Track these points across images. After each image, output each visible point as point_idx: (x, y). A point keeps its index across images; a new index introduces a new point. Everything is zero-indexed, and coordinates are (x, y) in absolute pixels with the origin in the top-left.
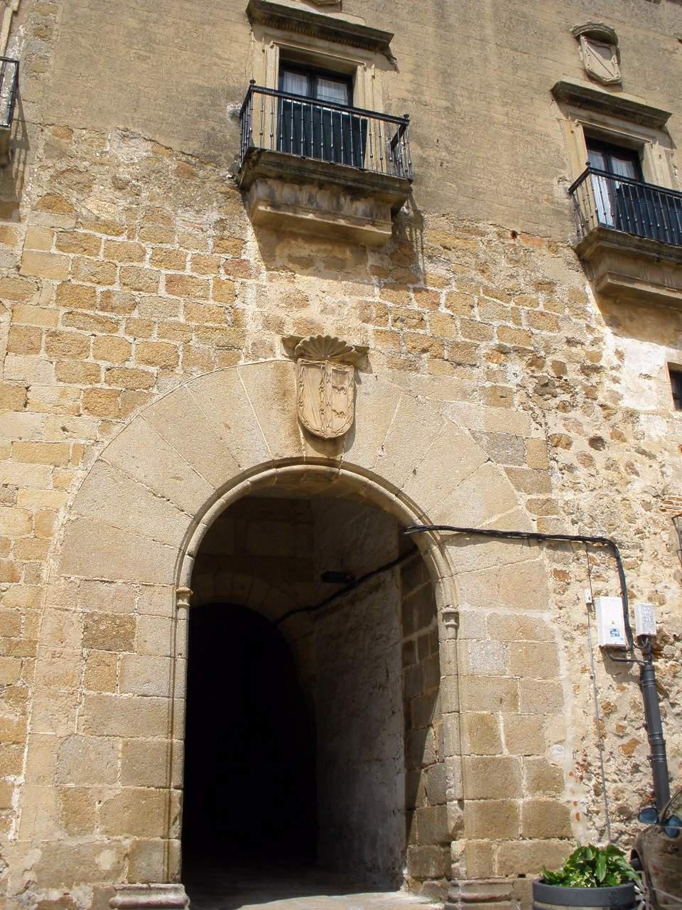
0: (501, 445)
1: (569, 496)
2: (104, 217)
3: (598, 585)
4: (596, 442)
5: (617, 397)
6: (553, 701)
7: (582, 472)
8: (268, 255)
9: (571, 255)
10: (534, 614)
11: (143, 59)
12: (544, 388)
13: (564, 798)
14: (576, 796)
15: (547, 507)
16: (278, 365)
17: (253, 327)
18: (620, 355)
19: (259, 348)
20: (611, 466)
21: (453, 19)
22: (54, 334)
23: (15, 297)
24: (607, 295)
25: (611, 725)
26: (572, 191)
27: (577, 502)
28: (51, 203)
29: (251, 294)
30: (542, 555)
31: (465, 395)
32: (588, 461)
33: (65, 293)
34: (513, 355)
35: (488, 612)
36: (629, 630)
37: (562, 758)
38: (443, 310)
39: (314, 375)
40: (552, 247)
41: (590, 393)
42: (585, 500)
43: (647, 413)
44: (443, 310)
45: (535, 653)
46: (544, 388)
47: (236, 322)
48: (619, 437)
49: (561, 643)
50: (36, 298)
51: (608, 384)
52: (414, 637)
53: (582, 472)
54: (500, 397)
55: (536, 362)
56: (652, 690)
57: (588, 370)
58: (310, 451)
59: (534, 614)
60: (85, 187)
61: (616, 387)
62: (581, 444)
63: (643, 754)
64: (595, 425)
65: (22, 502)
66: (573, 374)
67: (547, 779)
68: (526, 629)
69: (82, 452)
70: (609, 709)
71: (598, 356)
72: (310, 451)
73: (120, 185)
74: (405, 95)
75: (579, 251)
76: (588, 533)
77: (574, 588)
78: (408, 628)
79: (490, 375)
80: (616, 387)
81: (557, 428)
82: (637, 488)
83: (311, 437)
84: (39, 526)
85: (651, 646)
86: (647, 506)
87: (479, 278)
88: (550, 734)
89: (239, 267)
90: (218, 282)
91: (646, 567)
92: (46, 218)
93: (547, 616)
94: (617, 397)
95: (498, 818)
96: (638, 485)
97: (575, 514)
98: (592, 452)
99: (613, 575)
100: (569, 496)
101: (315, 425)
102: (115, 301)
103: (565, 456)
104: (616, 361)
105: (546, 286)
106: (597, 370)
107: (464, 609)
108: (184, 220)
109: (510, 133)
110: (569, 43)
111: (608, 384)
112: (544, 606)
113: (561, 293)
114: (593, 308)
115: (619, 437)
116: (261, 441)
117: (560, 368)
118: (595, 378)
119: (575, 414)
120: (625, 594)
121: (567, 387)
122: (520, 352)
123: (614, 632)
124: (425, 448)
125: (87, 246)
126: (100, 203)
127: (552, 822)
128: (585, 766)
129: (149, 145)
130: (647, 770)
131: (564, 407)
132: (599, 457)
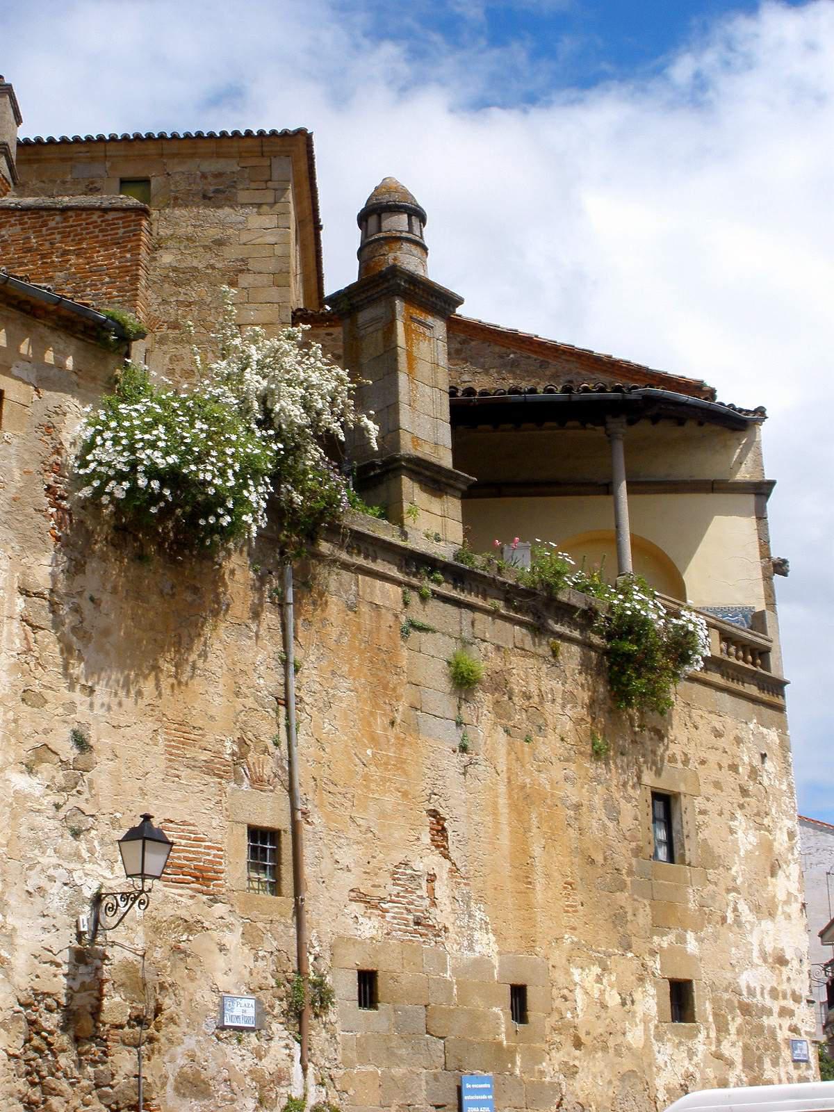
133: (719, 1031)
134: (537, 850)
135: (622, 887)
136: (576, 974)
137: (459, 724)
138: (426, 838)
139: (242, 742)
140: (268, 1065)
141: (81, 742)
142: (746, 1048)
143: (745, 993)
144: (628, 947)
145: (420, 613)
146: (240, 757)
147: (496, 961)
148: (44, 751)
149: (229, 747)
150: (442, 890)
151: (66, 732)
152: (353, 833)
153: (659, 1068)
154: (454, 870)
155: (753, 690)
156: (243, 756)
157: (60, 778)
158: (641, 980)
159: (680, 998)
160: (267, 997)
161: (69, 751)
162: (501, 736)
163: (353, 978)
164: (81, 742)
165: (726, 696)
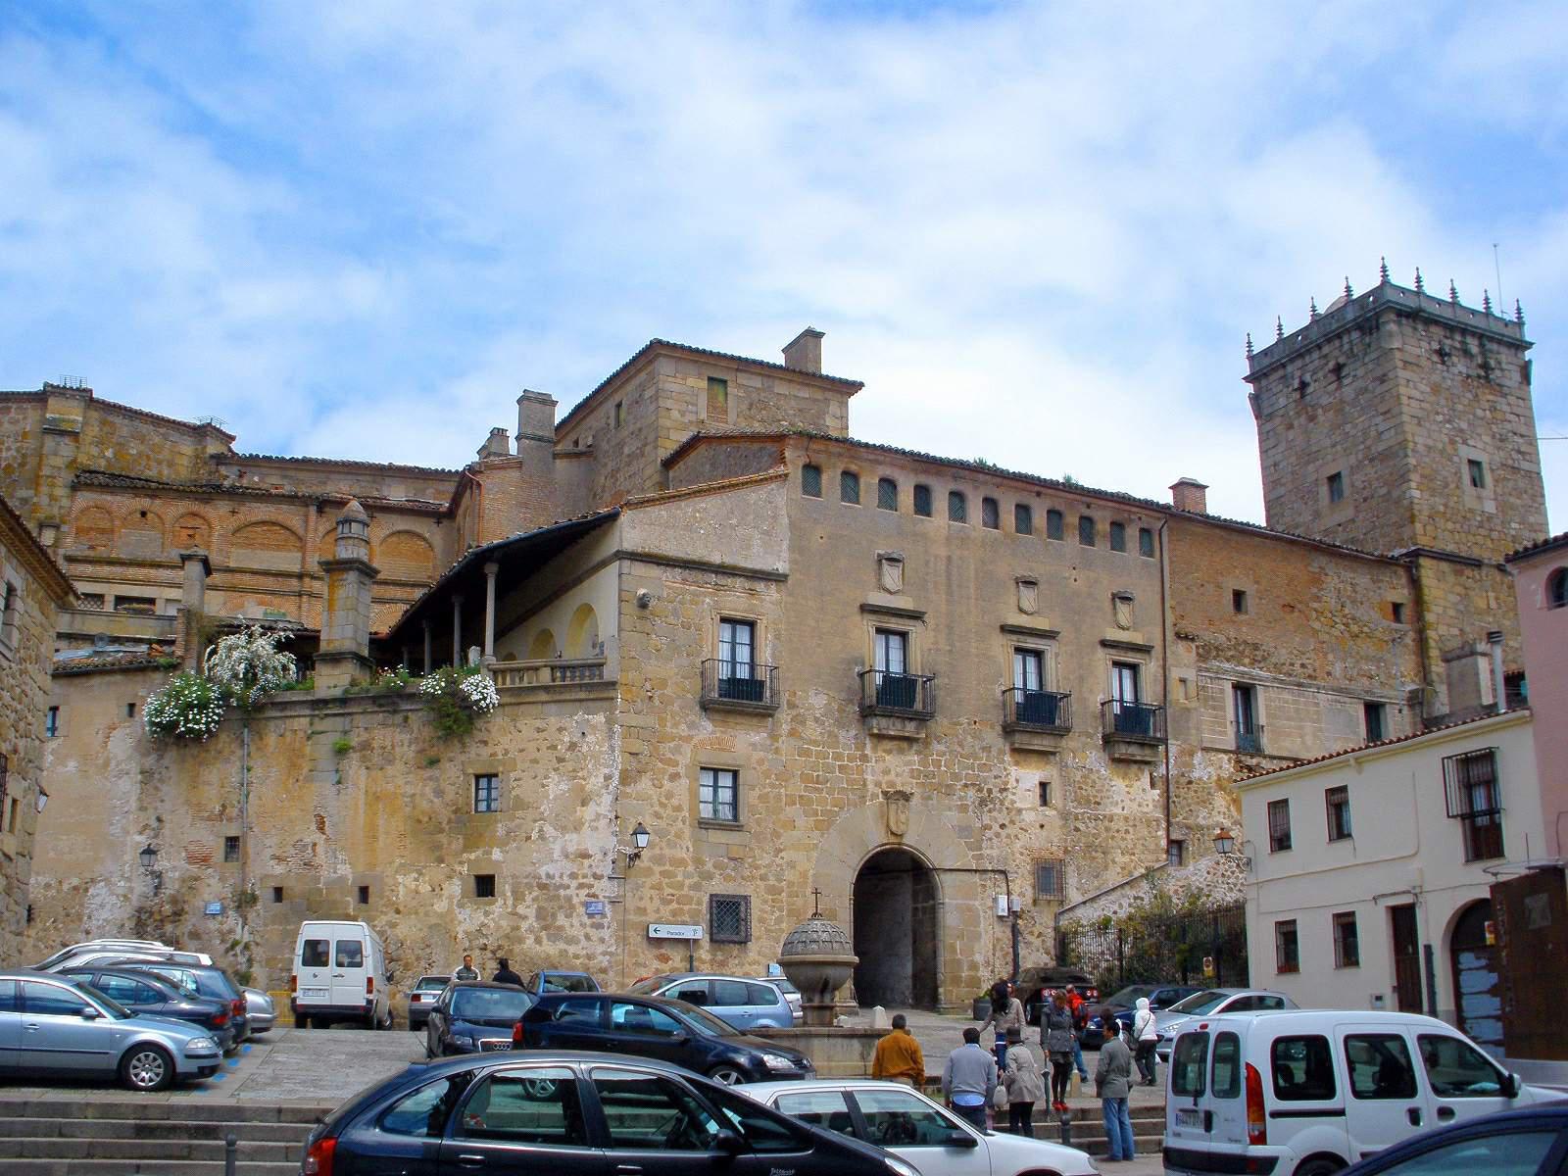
0: (964, 830)
1: (988, 852)
2: (813, 738)
3: (997, 890)
4: (1003, 826)
5: (1013, 802)
6: (977, 937)
7: (995, 840)
8: (874, 749)
9: (999, 729)
10: (971, 903)
11: (819, 645)
12: (983, 802)
13: (980, 974)
14: (984, 973)
15: (980, 857)
16: (881, 803)
17: (870, 786)
18: (1017, 781)
19: (874, 796)
20: (1008, 836)
21: (955, 587)
22: (801, 797)
23: (786, 781)
24: (1014, 750)
25: (998, 948)
26: (1004, 692)
27: (992, 853)
28: (792, 733)
29: (869, 770)
30: (976, 878)
31: (950, 809)
32: (998, 835)
33: (805, 778)
34: (971, 788)
35: (955, 902)
36: (1009, 909)
37: (979, 958)
38: (943, 768)
39: (893, 807)
40: (992, 727)
41: (1002, 804)
42: (995, 853)
43: (1026, 809)
44: (943, 768)
45: (971, 916)
46: (983, 802)
47: (865, 785)
48: (1012, 822)
49: (982, 914)
50: (792, 781)
51: (1010, 797)
52: (919, 906)
53: (995, 840)
54: (963, 808)
55: (980, 790)
56: (1015, 932)
57: (1003, 790)
58: (893, 839)
59: (971, 903)
60: (803, 723)
61: (1013, 797)
62: (996, 827)
63: (1010, 958)
64: (1003, 818)
65: (798, 868)
66: (996, 793)
67: (974, 966)
68: (970, 909)
69: (816, 845)
70: (998, 939)
71: (1007, 783)
72: (893, 839)
73: (816, 720)
74: (932, 646)
75: (1004, 728)
76: (996, 867)
77: (989, 891)
78: (915, 900)
79: (961, 798)
80: (1013, 797)
81: (987, 821)
82: (1018, 845)
83: (892, 833)
84: (804, 875)
85: (1014, 914)
86: (1022, 854)
87: (959, 749)
88: (976, 948)
89: (864, 758)
90: (858, 766)
91: (1018, 881)
92: (793, 741)
93: (977, 903)
94: (1013, 802)
95: (956, 980)
96: (1018, 845)
97: (991, 860)
98: (1000, 831)
99: (1004, 885)
100: (988, 852)
101: (894, 829)
102: (821, 778)
103: (989, 834)
104: (1015, 784)
105: (987, 749)
106: (1006, 790)
107: (947, 900)
108: (842, 733)
109: (976, 660)
110: (1012, 585)
111: (1010, 797)
112: (976, 899)
113: (994, 753)
114: (1007, 758)
115: (1012, 822)
116: (876, 839)
117: (990, 791)
118: (1005, 794)
119: (995, 814)
120: (1009, 894)
121: (992, 801)
122: (973, 785)
123: (1003, 910)
124: (930, 836)
125: (807, 753)
126: (812, 731)
127: (975, 982)
128: (988, 963)
129: (826, 697)
130: (1011, 964)
131: (990, 811)
132: (1003, 833)
133: (516, 899)
134: (381, 822)
135: (441, 831)
136: (400, 879)
137: (337, 771)
138: (314, 827)
139: (223, 806)
140: (225, 927)
141: (159, 820)
142: (540, 909)
143: (544, 877)
144: (442, 862)
145: (319, 726)
146: (222, 813)
147: (350, 877)
148: (146, 826)
149: (218, 808)
150: (320, 849)
151: (154, 818)
152: (273, 831)
153: (460, 922)
154: (328, 839)
155: (582, 695)
156: (224, 810)
157: (152, 834)
158: (450, 877)
159: (485, 886)
160: (226, 902)
161: (154, 824)
162: (363, 771)
163: (272, 891)
164: (159, 820)
165: (553, 705)
